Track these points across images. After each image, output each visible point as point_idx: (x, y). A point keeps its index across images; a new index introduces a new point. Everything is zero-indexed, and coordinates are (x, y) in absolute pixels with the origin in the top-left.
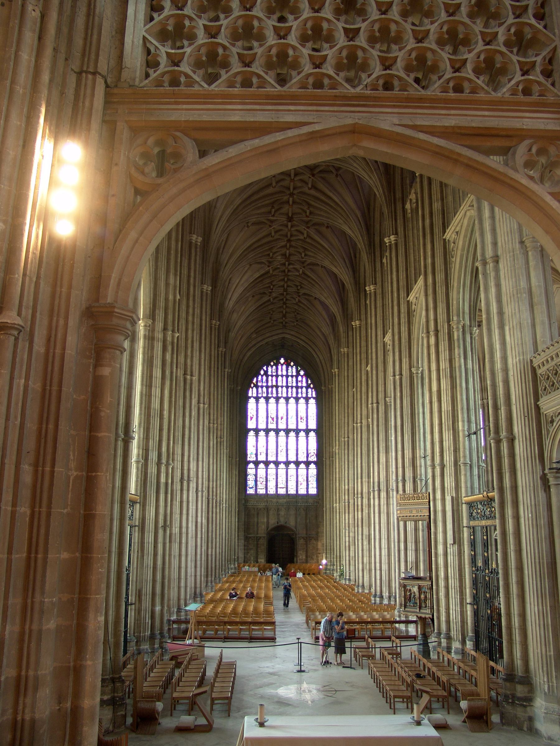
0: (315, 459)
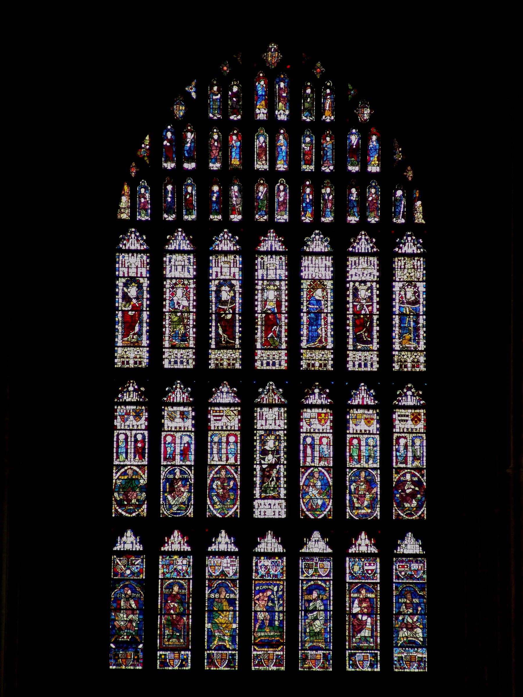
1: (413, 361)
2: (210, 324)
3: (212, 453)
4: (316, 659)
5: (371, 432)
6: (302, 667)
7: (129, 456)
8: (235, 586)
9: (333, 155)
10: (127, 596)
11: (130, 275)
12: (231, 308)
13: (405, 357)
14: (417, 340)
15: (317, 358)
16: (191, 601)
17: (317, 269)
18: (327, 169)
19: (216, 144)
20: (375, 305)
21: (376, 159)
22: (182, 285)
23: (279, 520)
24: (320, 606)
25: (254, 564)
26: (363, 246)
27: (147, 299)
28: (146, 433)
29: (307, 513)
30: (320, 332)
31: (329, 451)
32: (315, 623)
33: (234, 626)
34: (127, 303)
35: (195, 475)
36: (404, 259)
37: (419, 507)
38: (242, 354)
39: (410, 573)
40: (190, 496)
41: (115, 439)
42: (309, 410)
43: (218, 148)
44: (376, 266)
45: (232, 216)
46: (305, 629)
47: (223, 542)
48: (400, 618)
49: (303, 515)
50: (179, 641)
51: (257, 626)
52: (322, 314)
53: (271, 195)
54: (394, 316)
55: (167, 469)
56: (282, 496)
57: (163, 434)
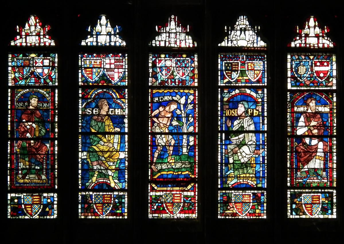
4: (243, 202)
6: (222, 214)
16: (56, 120)
25: (150, 65)
32: (241, 150)
33: (122, 155)
47: (104, 32)
51: (156, 155)
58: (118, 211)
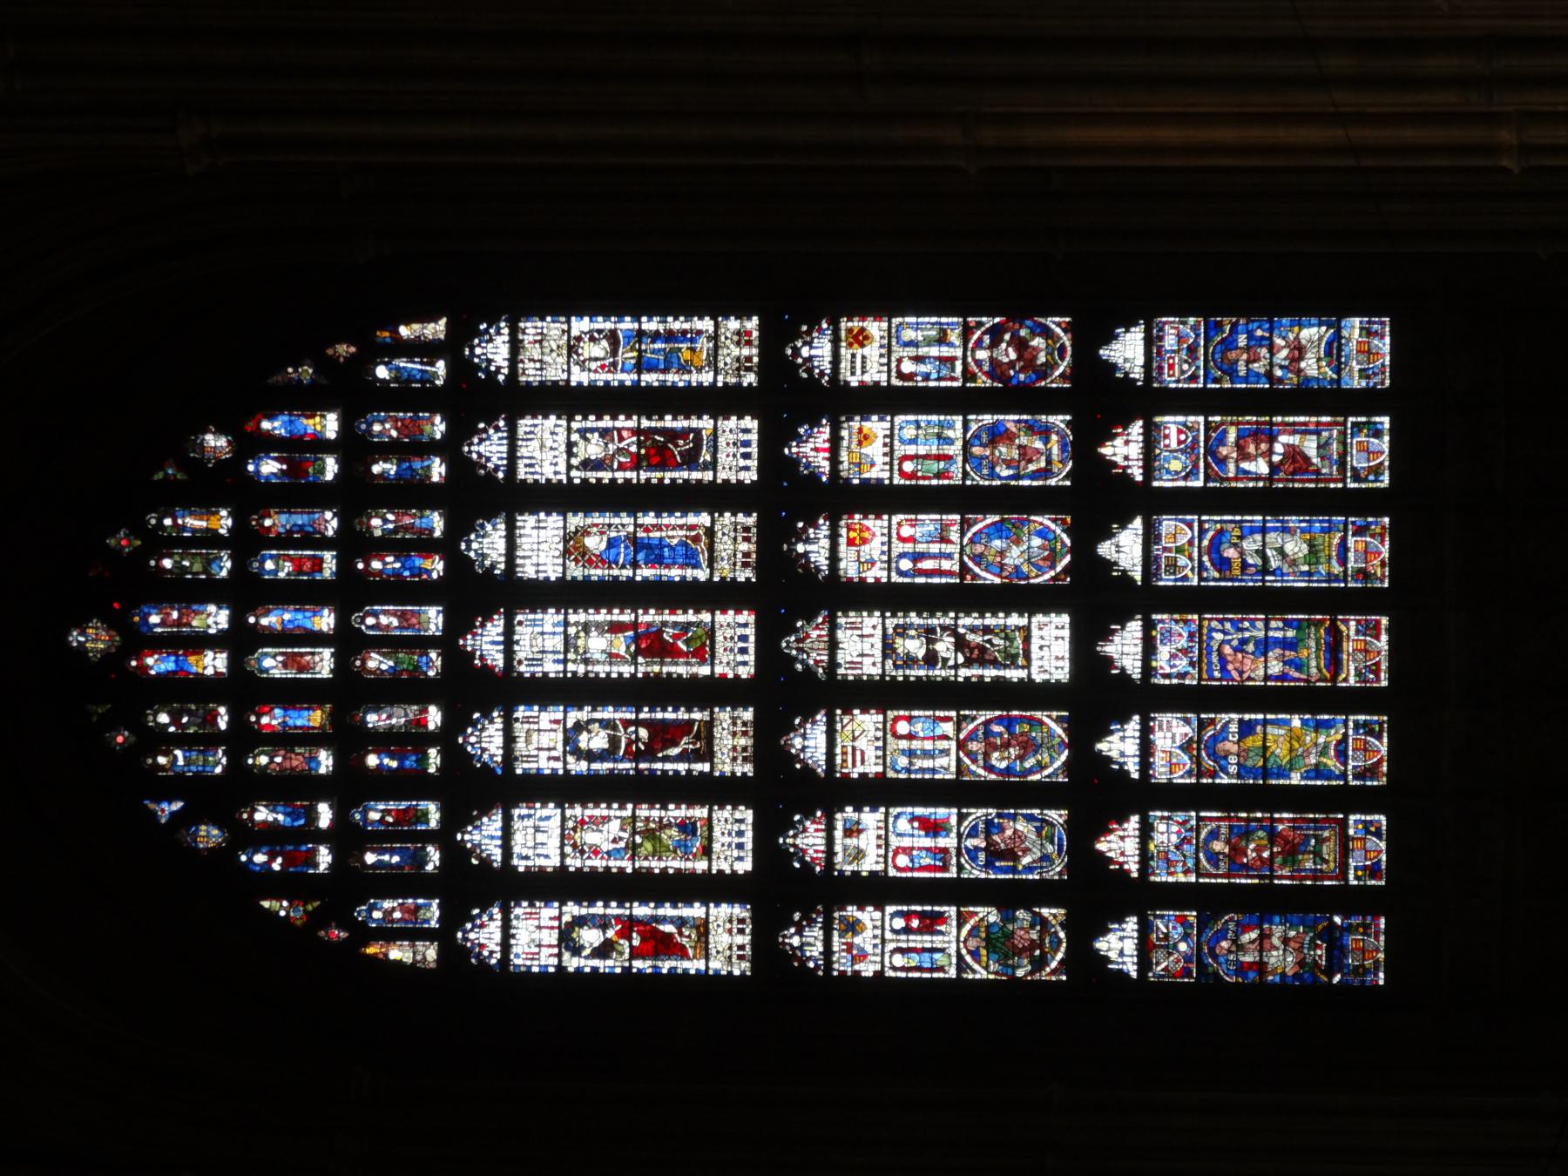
0: (1053, 323)
1: (738, 343)
2: (659, 773)
3: (933, 771)
4: (1366, 552)
5: (888, 432)
6: (1382, 581)
7: (939, 946)
8: (1213, 722)
9: (302, 513)
10: (1234, 949)
11: (556, 943)
12: (625, 728)
13: (728, 360)
14: (691, 336)
15: (732, 547)
16: (1244, 815)
17: (541, 547)
18: (331, 523)
19: (278, 760)
20: (618, 424)
21: (311, 422)
22: (575, 832)
23: (1074, 626)
24: (1255, 542)
26: (494, 449)
27: (606, 906)
28: (890, 909)
29: (1059, 569)
30: (675, 541)
31: (928, 522)
32: (1290, 553)
34: (613, 949)
35: (978, 805)
36: (522, 361)
37: (1046, 333)
38: (722, 707)
39: (1184, 352)
40: (1023, 815)
41: (902, 975)
42: (842, 565)
43: (288, 755)
44: (536, 422)
45: (431, 726)
46: (1303, 573)
47: (1121, 746)
48: (1278, 373)
49: (1063, 576)
50: (1328, 839)
51: (1297, 675)
52: (638, 535)
53: (387, 643)
54: (643, 384)
55: (967, 866)
56: (1023, 621)
57: (892, 872)
58: (1377, 729)
